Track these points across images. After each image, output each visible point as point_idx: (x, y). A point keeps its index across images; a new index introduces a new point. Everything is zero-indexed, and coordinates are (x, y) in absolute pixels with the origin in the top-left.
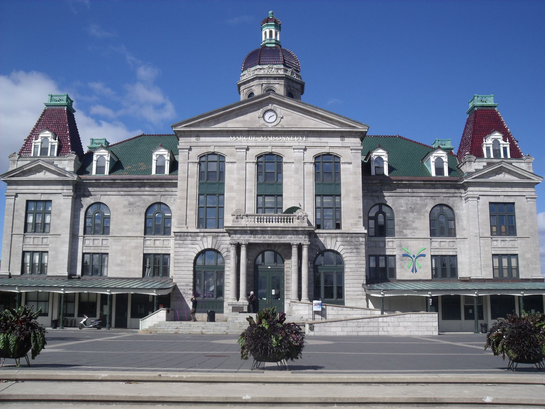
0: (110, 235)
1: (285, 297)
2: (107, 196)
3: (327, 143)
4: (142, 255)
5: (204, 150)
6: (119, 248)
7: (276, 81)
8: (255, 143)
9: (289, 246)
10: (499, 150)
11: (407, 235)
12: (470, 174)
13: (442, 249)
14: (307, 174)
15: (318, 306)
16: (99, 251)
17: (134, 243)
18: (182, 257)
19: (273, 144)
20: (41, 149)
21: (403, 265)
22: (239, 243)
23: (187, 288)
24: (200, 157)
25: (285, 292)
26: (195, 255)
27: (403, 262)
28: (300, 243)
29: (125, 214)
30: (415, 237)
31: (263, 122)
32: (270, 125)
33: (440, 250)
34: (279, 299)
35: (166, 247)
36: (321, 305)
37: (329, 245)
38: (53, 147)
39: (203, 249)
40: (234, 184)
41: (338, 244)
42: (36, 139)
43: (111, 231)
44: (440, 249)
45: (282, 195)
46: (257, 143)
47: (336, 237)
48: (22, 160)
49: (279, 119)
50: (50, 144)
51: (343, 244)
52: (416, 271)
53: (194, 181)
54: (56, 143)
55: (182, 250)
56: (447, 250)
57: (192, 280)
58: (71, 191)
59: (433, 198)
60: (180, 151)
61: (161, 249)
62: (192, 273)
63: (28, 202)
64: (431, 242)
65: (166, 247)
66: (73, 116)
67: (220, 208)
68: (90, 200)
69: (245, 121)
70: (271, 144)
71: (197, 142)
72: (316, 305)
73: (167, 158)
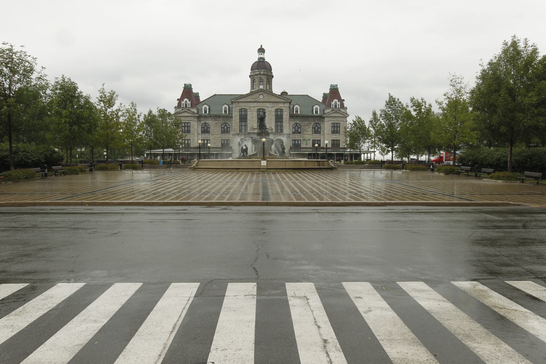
5: (241, 108)
6: (213, 138)
7: (263, 76)
10: (337, 105)
12: (326, 113)
16: (207, 139)
17: (218, 136)
19: (262, 106)
20: (185, 104)
38: (189, 104)
40: (250, 118)
42: (183, 101)
47: (281, 135)
54: (190, 103)
64: (313, 135)
66: (192, 90)
67: (246, 126)
69: (253, 98)
73: (228, 108)
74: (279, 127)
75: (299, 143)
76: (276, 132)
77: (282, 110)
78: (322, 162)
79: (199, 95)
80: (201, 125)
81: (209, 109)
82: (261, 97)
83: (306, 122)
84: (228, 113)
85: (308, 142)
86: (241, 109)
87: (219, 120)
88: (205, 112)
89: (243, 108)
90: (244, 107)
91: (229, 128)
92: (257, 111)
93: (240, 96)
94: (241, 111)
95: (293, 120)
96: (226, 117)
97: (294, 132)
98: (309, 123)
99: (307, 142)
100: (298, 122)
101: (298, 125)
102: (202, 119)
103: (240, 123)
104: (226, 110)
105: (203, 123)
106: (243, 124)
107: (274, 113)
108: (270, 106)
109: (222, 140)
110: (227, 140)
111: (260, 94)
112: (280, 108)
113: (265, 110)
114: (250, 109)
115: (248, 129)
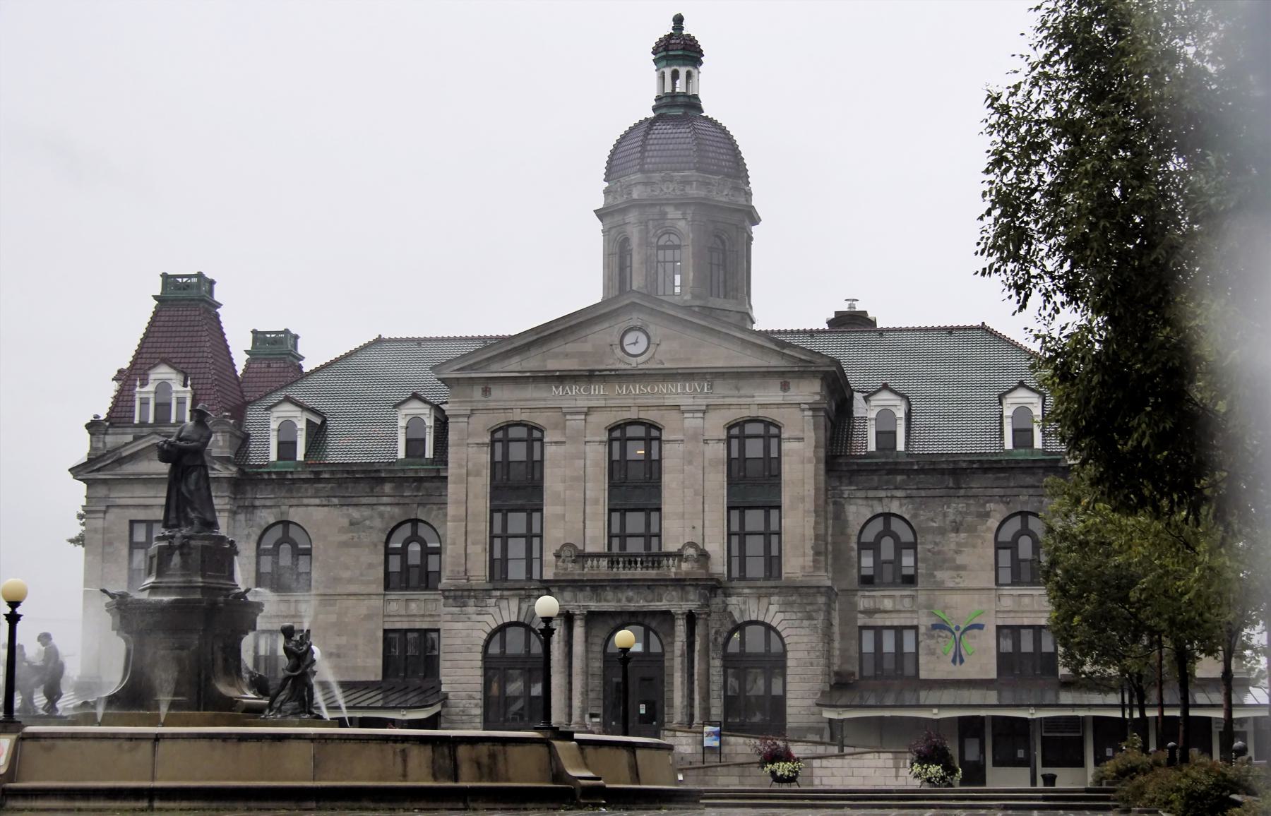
0: (314, 592)
1: (666, 720)
2: (304, 508)
3: (753, 397)
4: (380, 634)
5: (500, 418)
6: (333, 618)
8: (604, 402)
9: (667, 616)
11: (943, 582)
13: (1023, 612)
14: (710, 464)
15: (714, 737)
17: (363, 607)
18: (459, 641)
19: (640, 402)
20: (157, 405)
21: (932, 647)
22: (568, 612)
23: (470, 704)
24: (493, 433)
25: (666, 709)
26: (485, 636)
27: (933, 641)
28: (690, 611)
29: (345, 544)
30: (961, 585)
31: (618, 352)
32: (634, 362)
33: (1019, 615)
34: (654, 723)
35: (431, 616)
36: (719, 735)
37: (754, 612)
38: (181, 402)
39: (500, 622)
40: (560, 487)
41: (773, 608)
42: (143, 385)
43: (313, 583)
44: (1015, 612)
45: (659, 510)
46: (608, 402)
47: (769, 595)
48: (113, 434)
49: (652, 347)
50: (174, 395)
51: (786, 606)
52: (962, 661)
53: (481, 485)
55: (459, 625)
56: (1033, 615)
57: (480, 687)
58: (227, 500)
59: (1004, 499)
60: (450, 420)
61: (421, 619)
62: (480, 672)
63: (132, 522)
64: (999, 597)
65: (431, 616)
66: (217, 316)
68: (266, 515)
69: (582, 355)
70: (637, 401)
71: (486, 401)
72: (709, 734)
73: (429, 422)
74: (755, 545)
75: (909, 647)
76: (735, 573)
77: (771, 431)
78: (483, 749)
79: (301, 351)
80: (255, 537)
81: (317, 434)
82: (636, 344)
83: (954, 509)
84: (429, 453)
85: (968, 645)
86: (506, 427)
87: (373, 500)
88: (287, 448)
89: (517, 418)
90: (517, 416)
91: (438, 552)
92: (611, 441)
93: (480, 345)
94: (506, 441)
95: (861, 494)
96: (420, 480)
97: (870, 572)
98: (973, 509)
99: (958, 643)
100: (895, 507)
101: (896, 525)
102: (263, 496)
103: (498, 517)
104: (421, 437)
105: (272, 521)
106: (517, 522)
107: (722, 448)
108: (690, 401)
109: (386, 631)
110: (424, 632)
111: (632, 323)
112: (761, 413)
113: (660, 430)
114: (562, 426)
115: (549, 557)
